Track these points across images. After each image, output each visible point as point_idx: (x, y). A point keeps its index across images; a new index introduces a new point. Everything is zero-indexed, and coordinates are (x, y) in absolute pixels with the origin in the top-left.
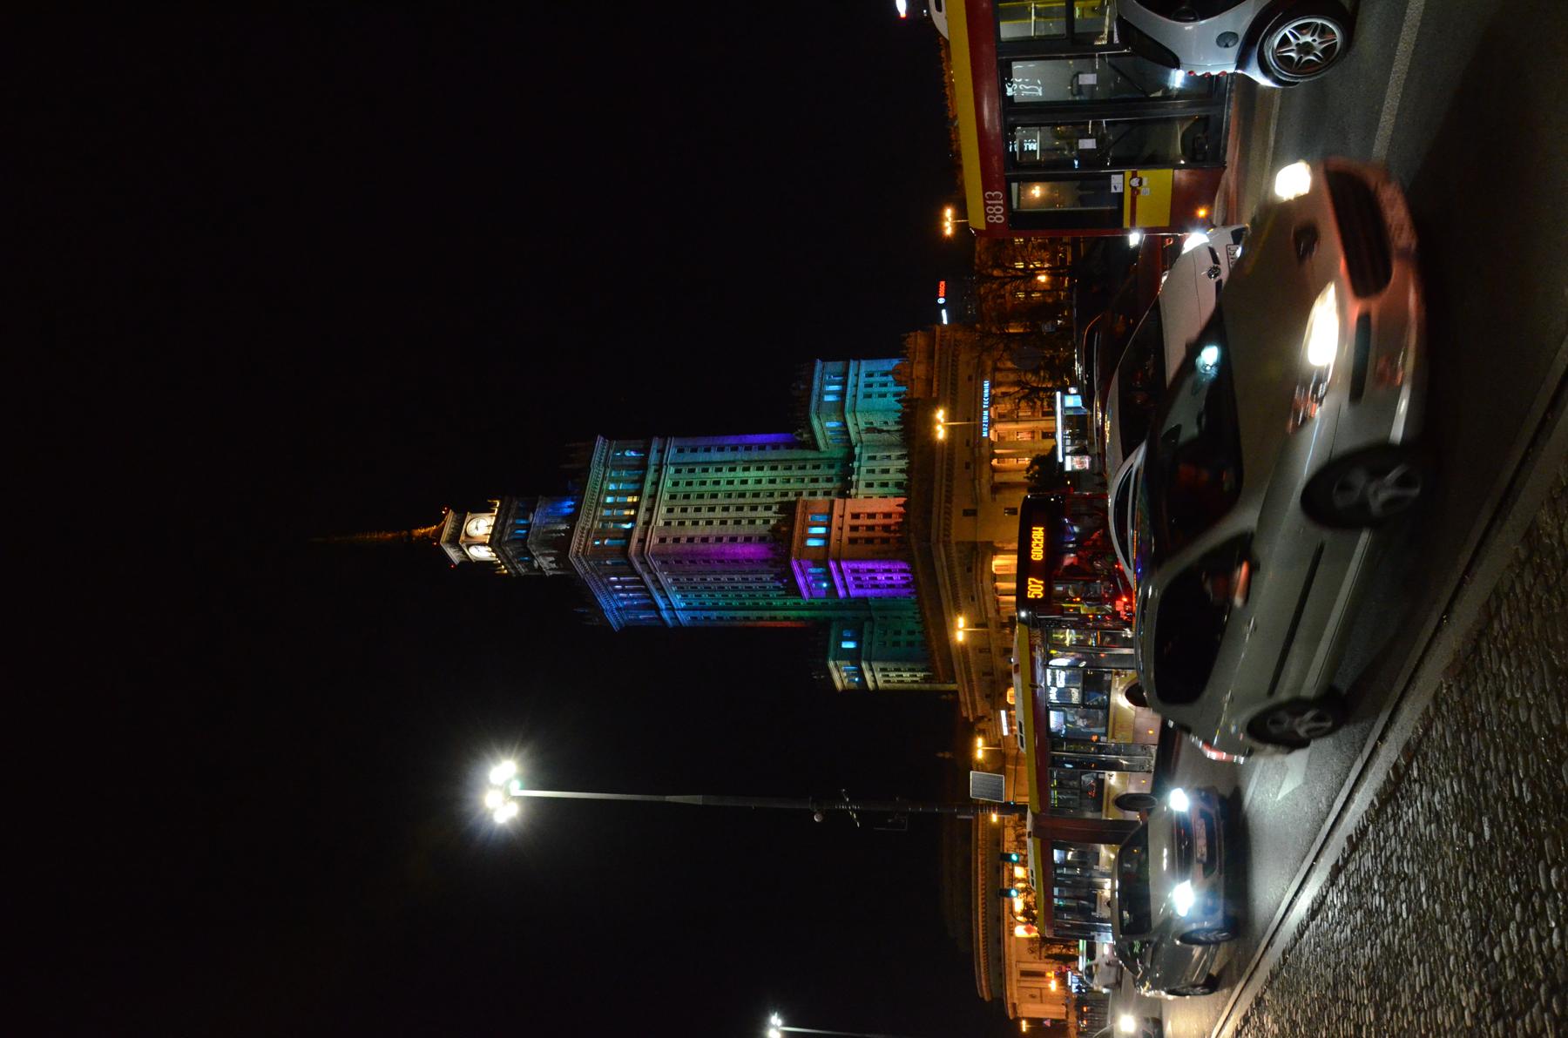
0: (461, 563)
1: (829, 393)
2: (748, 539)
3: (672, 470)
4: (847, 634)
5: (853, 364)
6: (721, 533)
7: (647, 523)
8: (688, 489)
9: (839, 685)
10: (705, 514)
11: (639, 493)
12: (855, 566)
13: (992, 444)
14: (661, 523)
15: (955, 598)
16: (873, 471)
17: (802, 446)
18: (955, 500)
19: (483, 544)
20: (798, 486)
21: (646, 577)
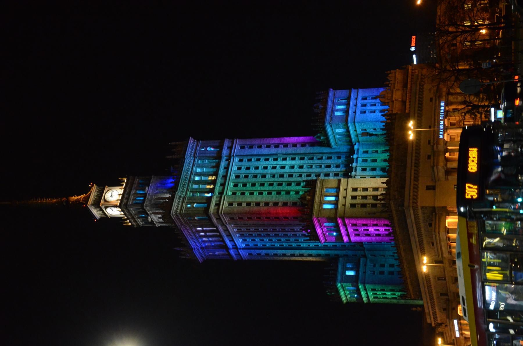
0: (101, 218)
1: (338, 110)
2: (285, 204)
3: (237, 159)
4: (349, 266)
5: (353, 92)
7: (221, 193)
8: (247, 171)
9: (344, 299)
10: (258, 188)
11: (216, 174)
12: (354, 221)
13: (446, 143)
14: (230, 193)
15: (421, 243)
16: (366, 161)
17: (321, 144)
18: (420, 178)
19: (116, 206)
20: (318, 170)
21: (220, 228)
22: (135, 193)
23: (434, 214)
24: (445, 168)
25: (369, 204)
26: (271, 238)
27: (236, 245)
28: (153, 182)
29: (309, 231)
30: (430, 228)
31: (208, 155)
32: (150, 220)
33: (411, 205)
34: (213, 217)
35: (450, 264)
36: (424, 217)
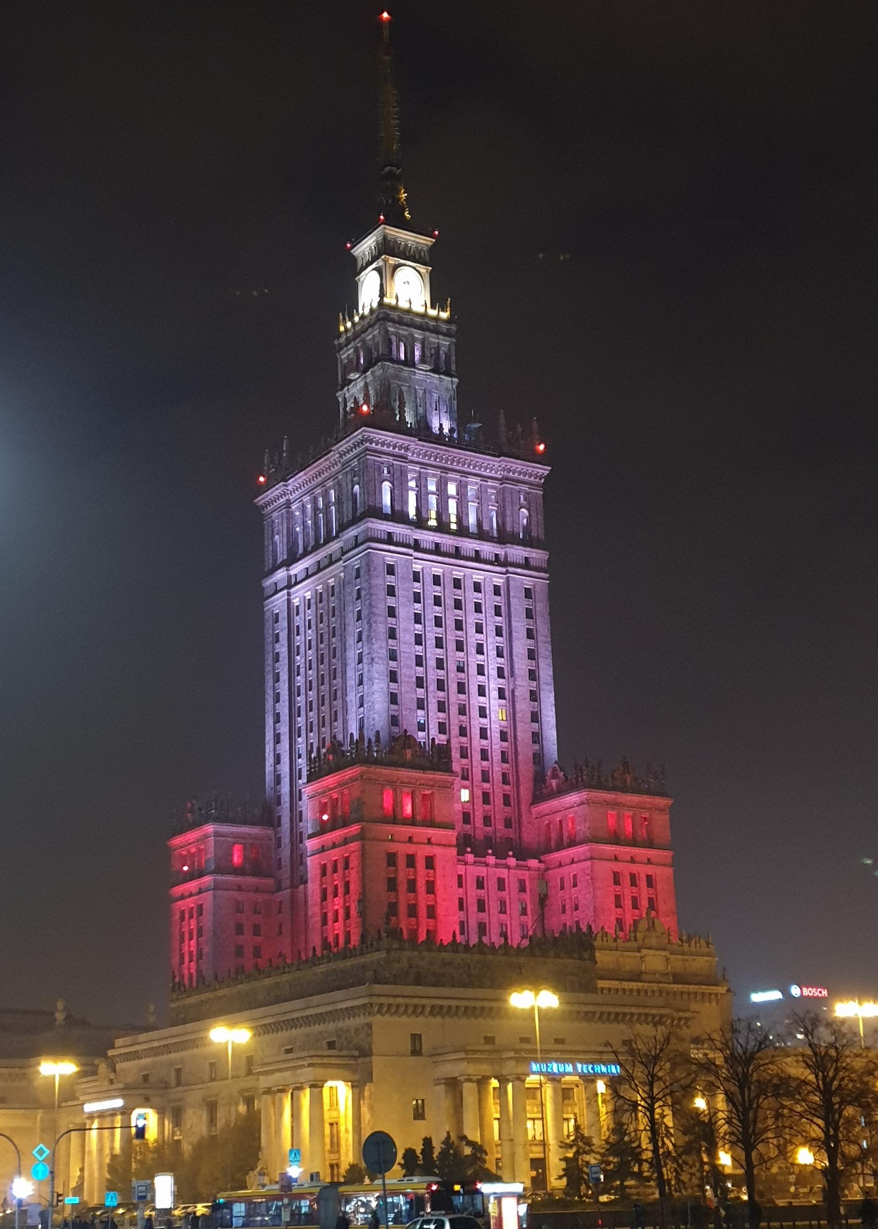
0: (354, 259)
3: (499, 581)
6: (402, 657)
7: (417, 546)
8: (471, 607)
12: (354, 863)
13: (520, 1079)
14: (417, 567)
15: (276, 1027)
18: (439, 1020)
19: (382, 294)
22: (414, 340)
23: (357, 1053)
24: (462, 1078)
25: (397, 898)
26: (314, 665)
27: (296, 583)
28: (441, 380)
29: (331, 757)
30: (324, 1044)
31: (508, 513)
32: (353, 376)
33: (375, 1000)
34: (359, 530)
35: (248, 1090)
36: (348, 1031)
